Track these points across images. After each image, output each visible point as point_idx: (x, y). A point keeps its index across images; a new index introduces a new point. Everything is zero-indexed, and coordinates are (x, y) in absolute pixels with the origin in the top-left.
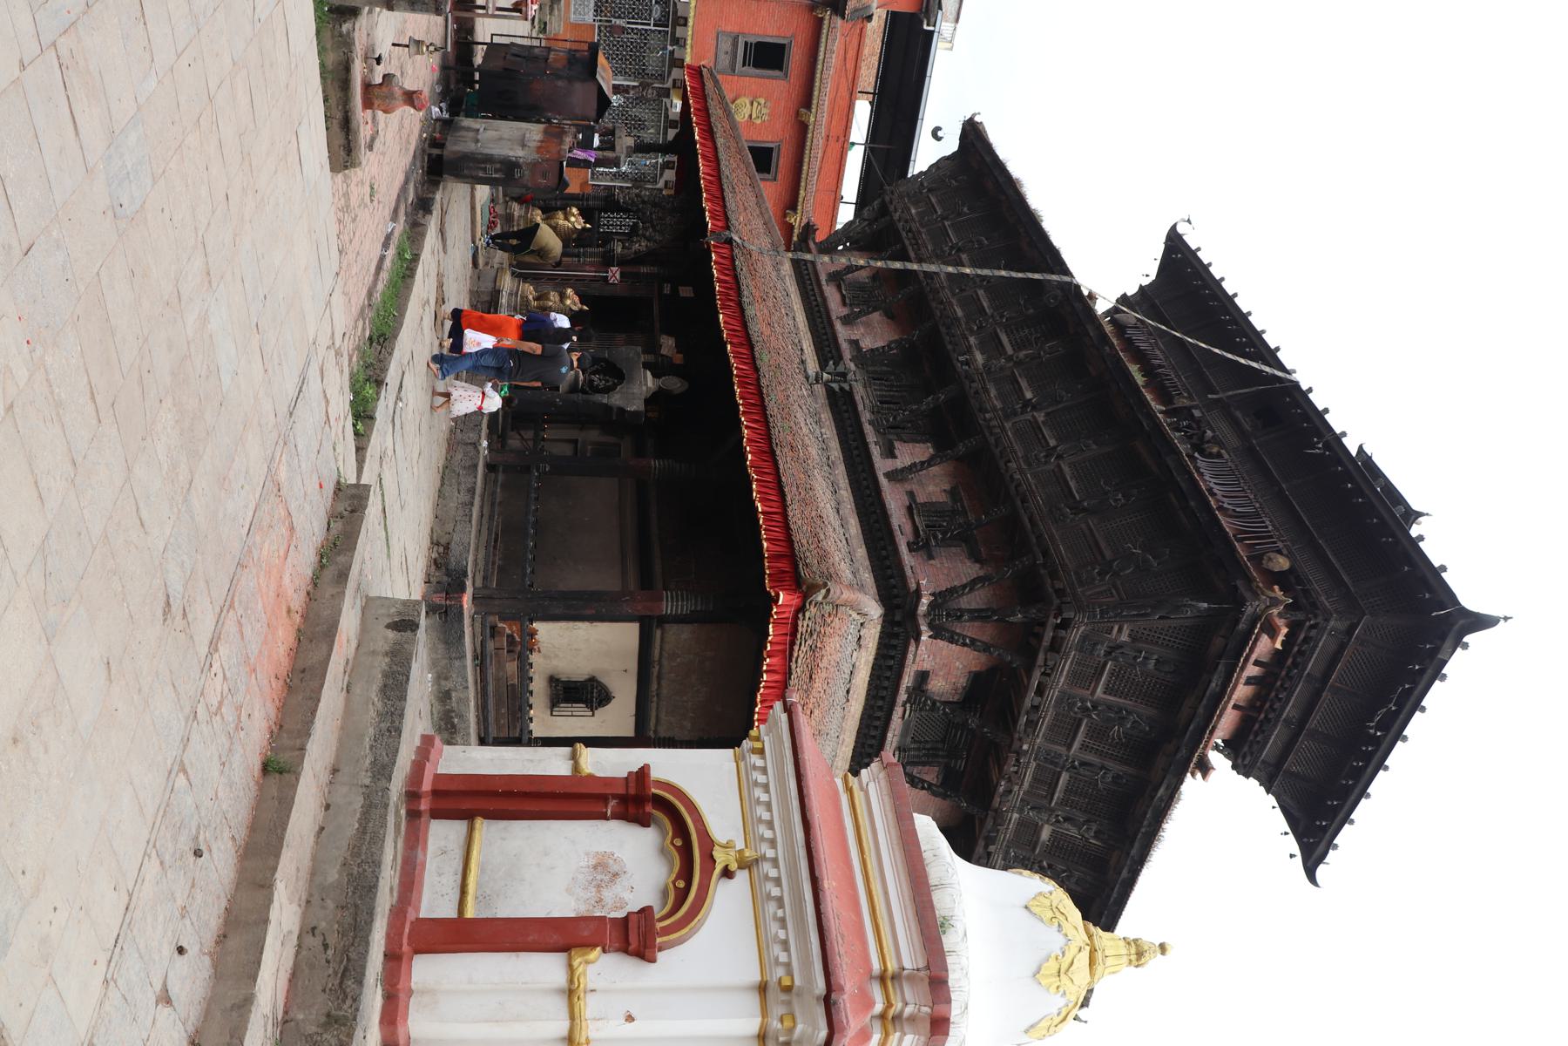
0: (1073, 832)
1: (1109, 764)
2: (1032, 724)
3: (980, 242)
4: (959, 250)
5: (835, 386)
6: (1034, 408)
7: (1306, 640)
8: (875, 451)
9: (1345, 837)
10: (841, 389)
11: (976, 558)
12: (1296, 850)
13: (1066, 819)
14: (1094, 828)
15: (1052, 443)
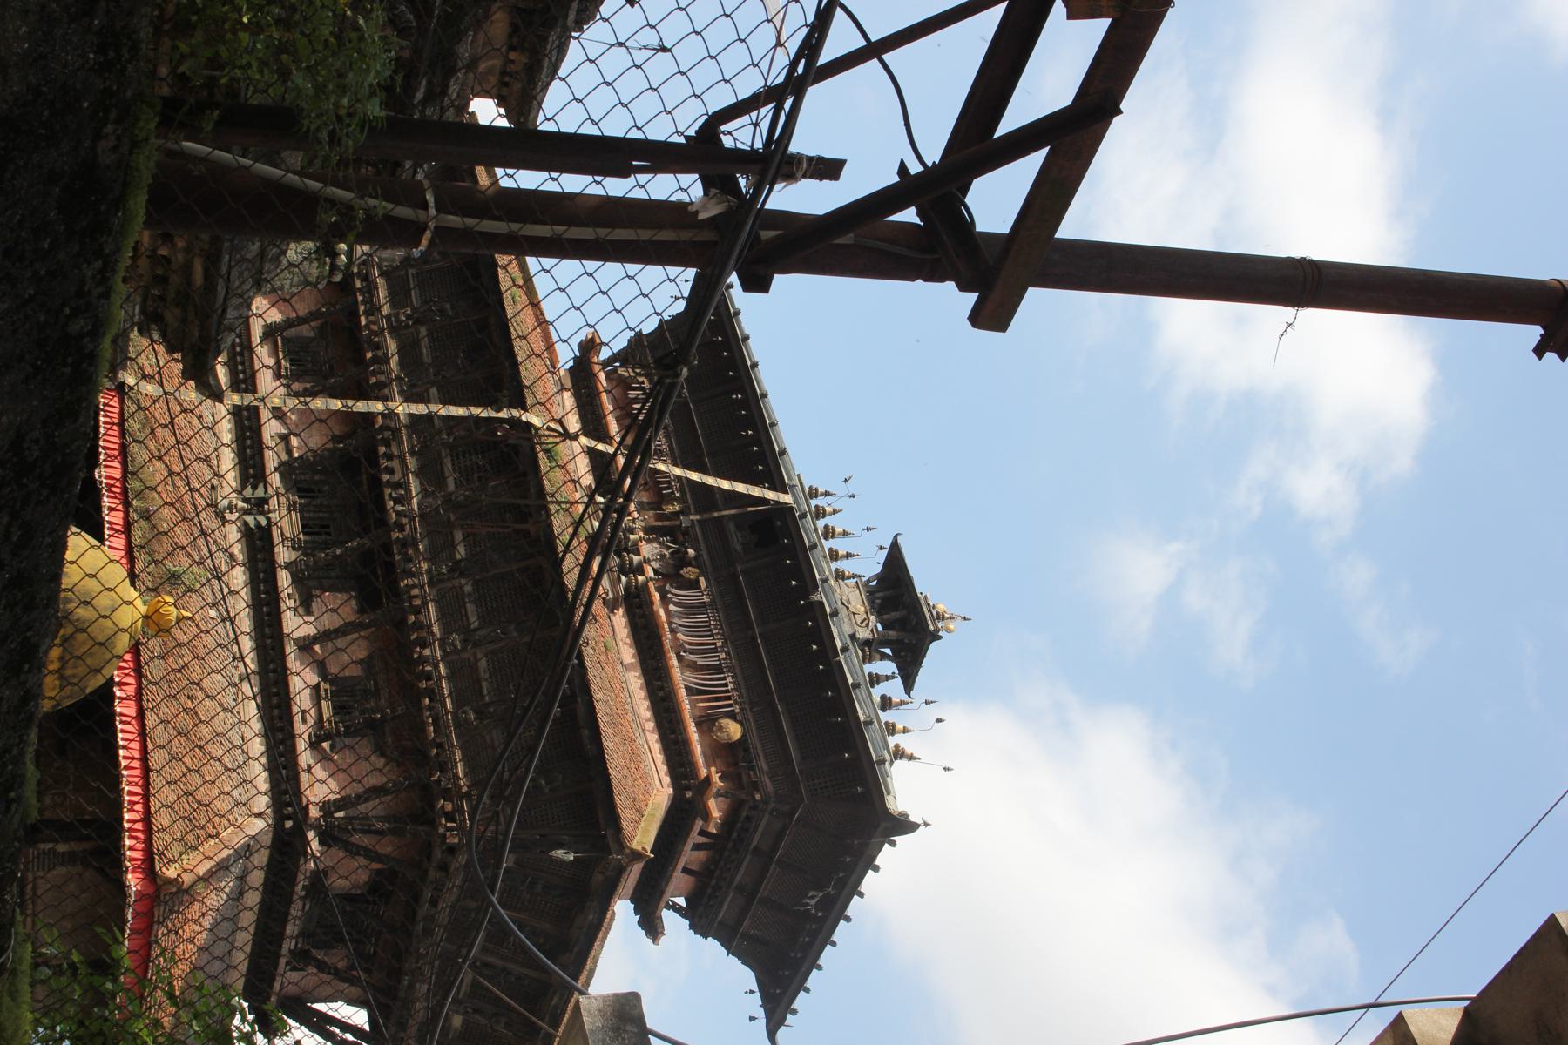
0: (484, 1021)
1: (511, 966)
2: (428, 932)
3: (442, 311)
4: (417, 322)
5: (250, 519)
6: (462, 575)
7: (748, 818)
8: (287, 603)
9: (801, 1000)
10: (258, 524)
11: (380, 750)
12: (760, 1013)
13: (476, 1011)
14: (504, 1020)
15: (474, 621)
